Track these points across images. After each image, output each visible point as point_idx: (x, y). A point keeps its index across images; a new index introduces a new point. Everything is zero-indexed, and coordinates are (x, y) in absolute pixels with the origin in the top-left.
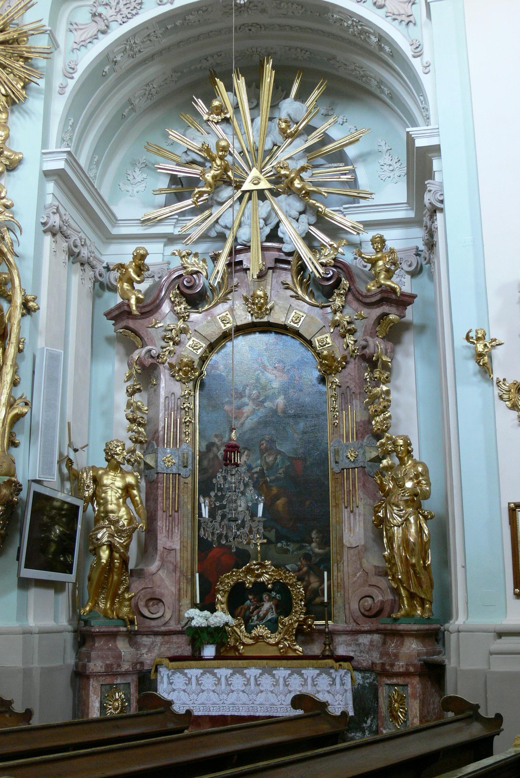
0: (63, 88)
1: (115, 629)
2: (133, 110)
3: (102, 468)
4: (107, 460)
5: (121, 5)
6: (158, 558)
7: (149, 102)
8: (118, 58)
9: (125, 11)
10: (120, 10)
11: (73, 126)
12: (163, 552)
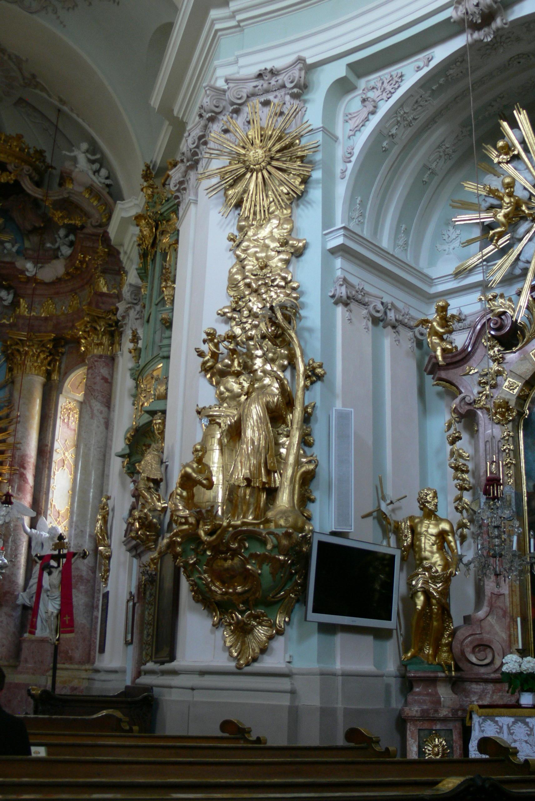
0: (343, 172)
1: (432, 675)
2: (433, 173)
3: (418, 517)
4: (421, 509)
5: (385, 85)
6: (486, 603)
7: (450, 163)
8: (394, 131)
9: (389, 88)
10: (384, 89)
11: (363, 204)
12: (491, 597)
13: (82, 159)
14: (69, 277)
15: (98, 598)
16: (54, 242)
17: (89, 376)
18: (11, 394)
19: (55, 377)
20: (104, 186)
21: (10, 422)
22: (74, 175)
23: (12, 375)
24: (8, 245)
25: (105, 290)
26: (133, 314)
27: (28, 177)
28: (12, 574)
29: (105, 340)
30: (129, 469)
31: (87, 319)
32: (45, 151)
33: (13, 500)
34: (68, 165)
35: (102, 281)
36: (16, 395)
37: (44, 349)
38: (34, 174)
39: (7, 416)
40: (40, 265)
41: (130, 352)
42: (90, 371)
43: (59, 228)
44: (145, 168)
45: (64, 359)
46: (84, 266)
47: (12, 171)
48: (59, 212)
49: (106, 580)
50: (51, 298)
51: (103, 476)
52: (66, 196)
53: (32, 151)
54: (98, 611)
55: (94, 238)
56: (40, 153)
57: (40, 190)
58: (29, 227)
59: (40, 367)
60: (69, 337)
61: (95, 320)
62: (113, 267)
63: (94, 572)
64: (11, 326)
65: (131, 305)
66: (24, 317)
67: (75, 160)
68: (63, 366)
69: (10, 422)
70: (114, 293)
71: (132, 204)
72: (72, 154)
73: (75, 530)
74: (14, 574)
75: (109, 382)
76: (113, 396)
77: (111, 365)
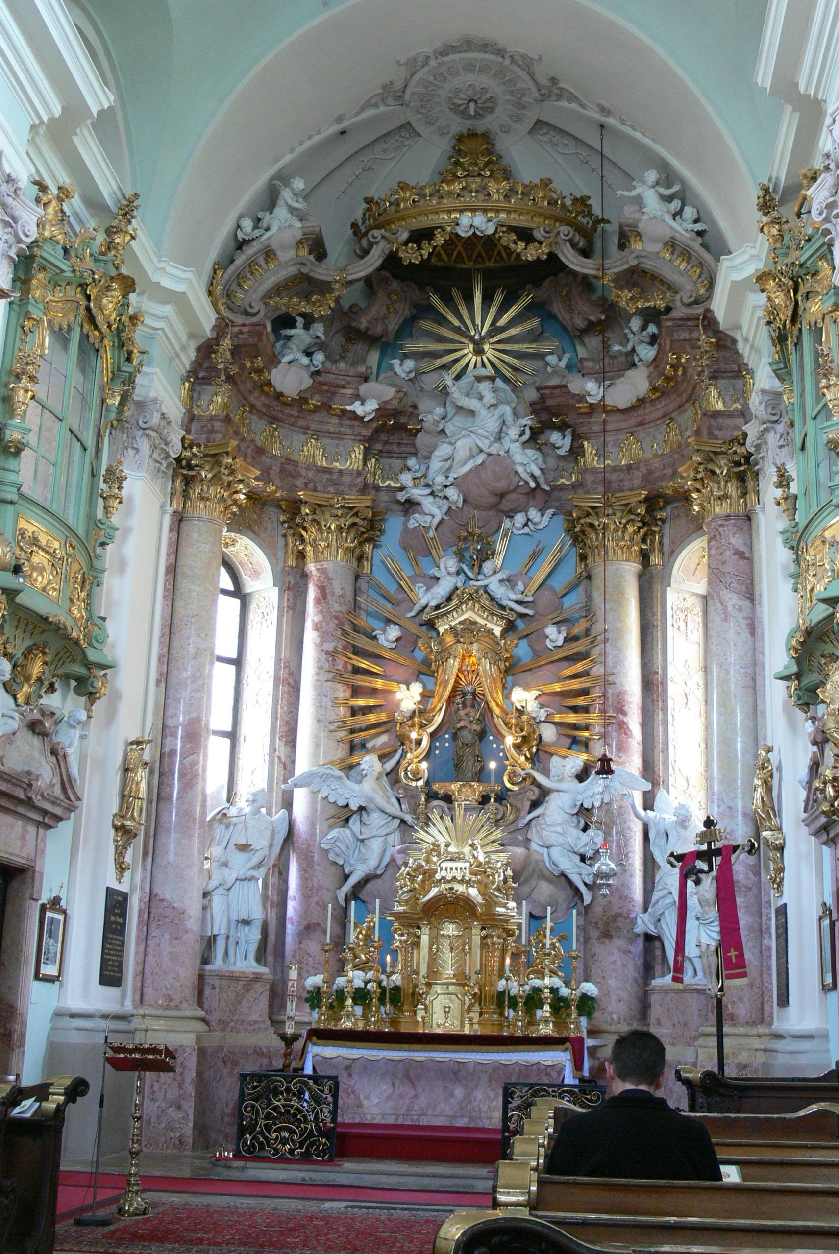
13: (651, 198)
14: (658, 394)
15: (768, 914)
16: (625, 340)
17: (713, 552)
18: (589, 598)
19: (655, 559)
20: (694, 234)
21: (592, 642)
22: (641, 228)
23: (586, 565)
24: (552, 359)
25: (720, 406)
26: (772, 439)
27: (568, 245)
28: (623, 885)
29: (732, 489)
30: (799, 698)
31: (697, 458)
32: (589, 198)
33: (613, 766)
34: (629, 213)
35: (714, 393)
36: (597, 597)
37: (632, 517)
38: (577, 238)
39: (587, 633)
40: (607, 382)
41: (778, 504)
42: (713, 543)
43: (629, 317)
44: (761, 193)
45: (667, 526)
46: (680, 373)
47: (542, 239)
48: (626, 292)
49: (780, 884)
50: (632, 434)
51: (756, 713)
52: (634, 263)
53: (568, 202)
54: (770, 937)
55: (689, 323)
56: (582, 201)
57: (590, 261)
58: (580, 324)
59: (629, 548)
60: (670, 492)
61: (711, 457)
62: (728, 364)
63: (758, 874)
64: (574, 487)
65: (769, 425)
66: (593, 470)
67: (639, 201)
68: (666, 541)
69: (592, 642)
70: (736, 410)
71: (747, 256)
72: (634, 193)
73: (719, 806)
74: (627, 885)
75: (746, 557)
76: (756, 580)
77: (746, 529)
